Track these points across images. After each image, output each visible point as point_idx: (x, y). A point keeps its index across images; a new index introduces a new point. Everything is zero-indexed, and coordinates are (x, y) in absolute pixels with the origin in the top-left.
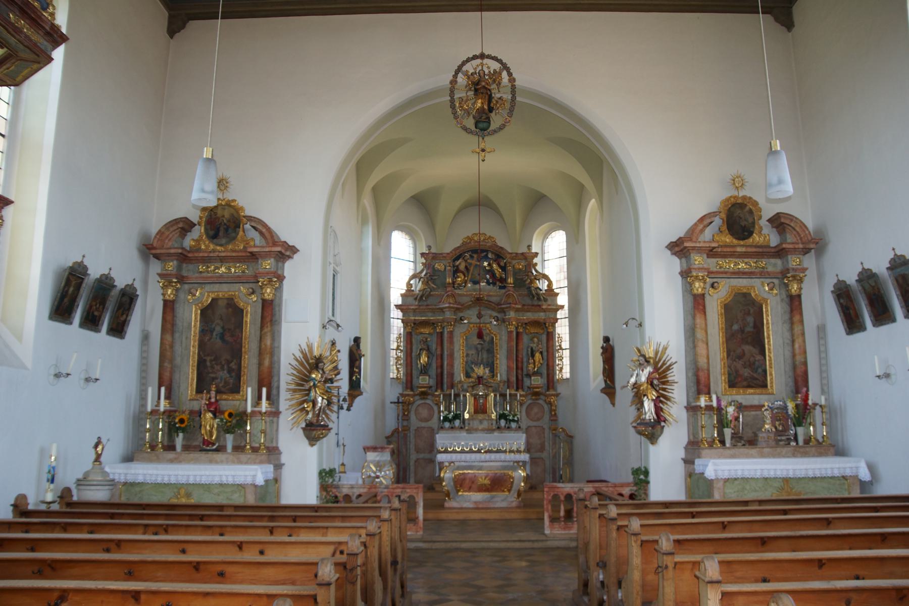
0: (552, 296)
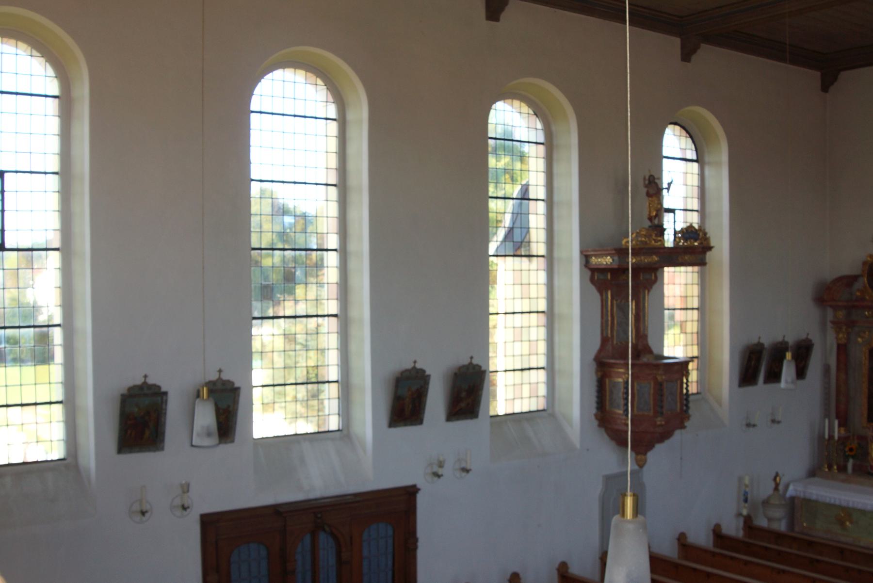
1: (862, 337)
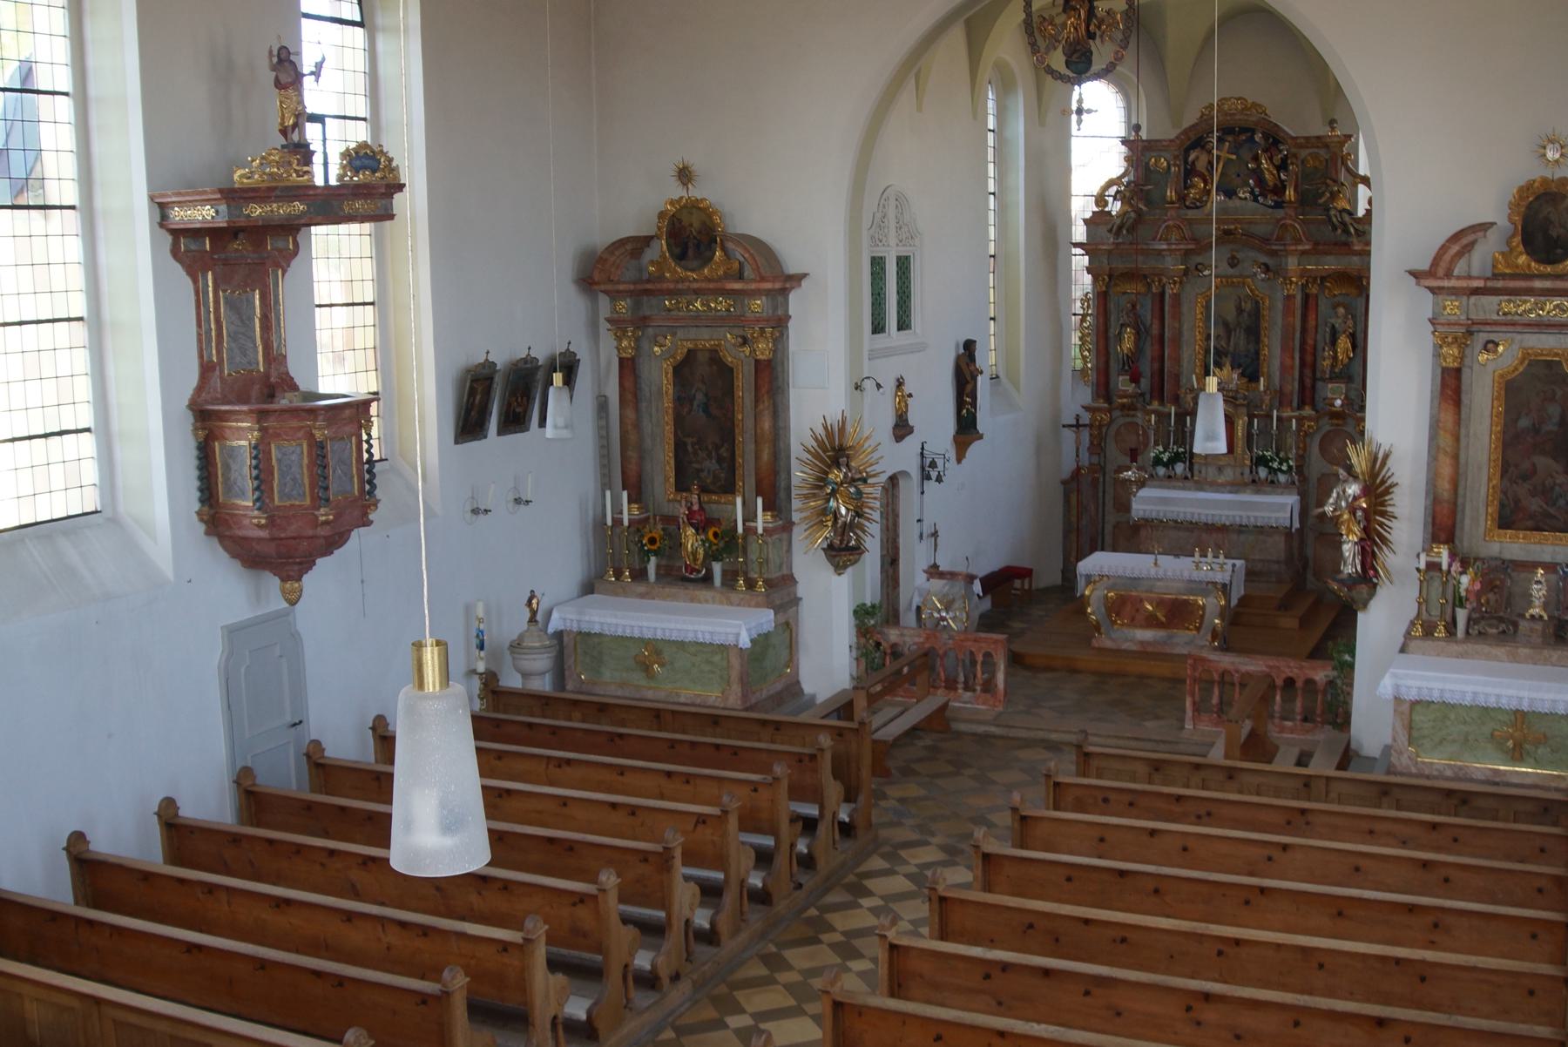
1: (660, 346)
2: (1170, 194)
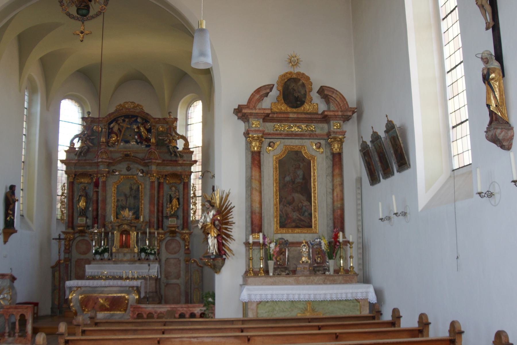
0: (187, 153)
2: (103, 139)
